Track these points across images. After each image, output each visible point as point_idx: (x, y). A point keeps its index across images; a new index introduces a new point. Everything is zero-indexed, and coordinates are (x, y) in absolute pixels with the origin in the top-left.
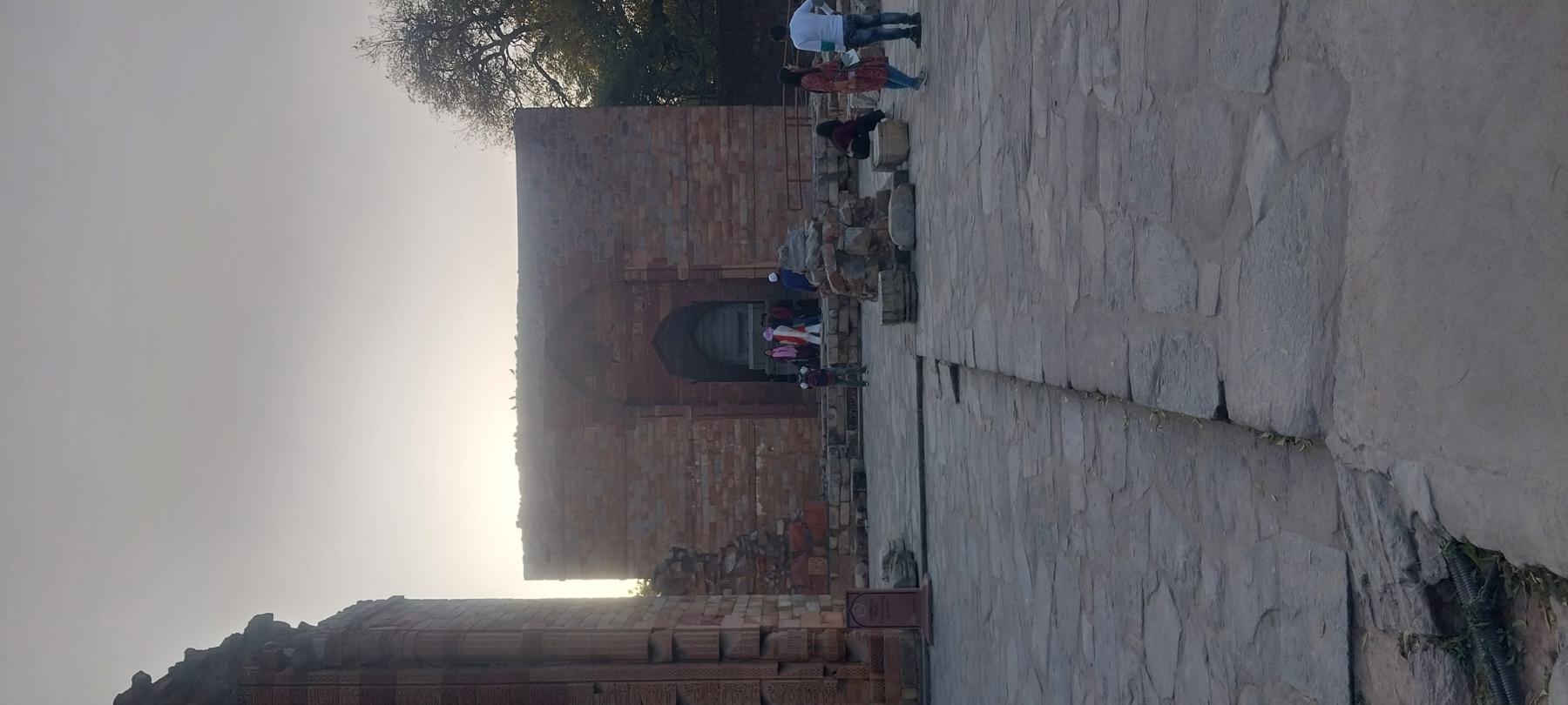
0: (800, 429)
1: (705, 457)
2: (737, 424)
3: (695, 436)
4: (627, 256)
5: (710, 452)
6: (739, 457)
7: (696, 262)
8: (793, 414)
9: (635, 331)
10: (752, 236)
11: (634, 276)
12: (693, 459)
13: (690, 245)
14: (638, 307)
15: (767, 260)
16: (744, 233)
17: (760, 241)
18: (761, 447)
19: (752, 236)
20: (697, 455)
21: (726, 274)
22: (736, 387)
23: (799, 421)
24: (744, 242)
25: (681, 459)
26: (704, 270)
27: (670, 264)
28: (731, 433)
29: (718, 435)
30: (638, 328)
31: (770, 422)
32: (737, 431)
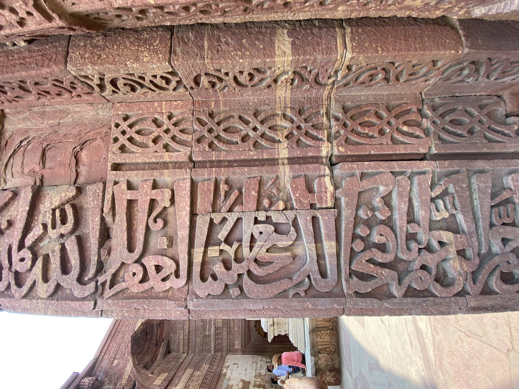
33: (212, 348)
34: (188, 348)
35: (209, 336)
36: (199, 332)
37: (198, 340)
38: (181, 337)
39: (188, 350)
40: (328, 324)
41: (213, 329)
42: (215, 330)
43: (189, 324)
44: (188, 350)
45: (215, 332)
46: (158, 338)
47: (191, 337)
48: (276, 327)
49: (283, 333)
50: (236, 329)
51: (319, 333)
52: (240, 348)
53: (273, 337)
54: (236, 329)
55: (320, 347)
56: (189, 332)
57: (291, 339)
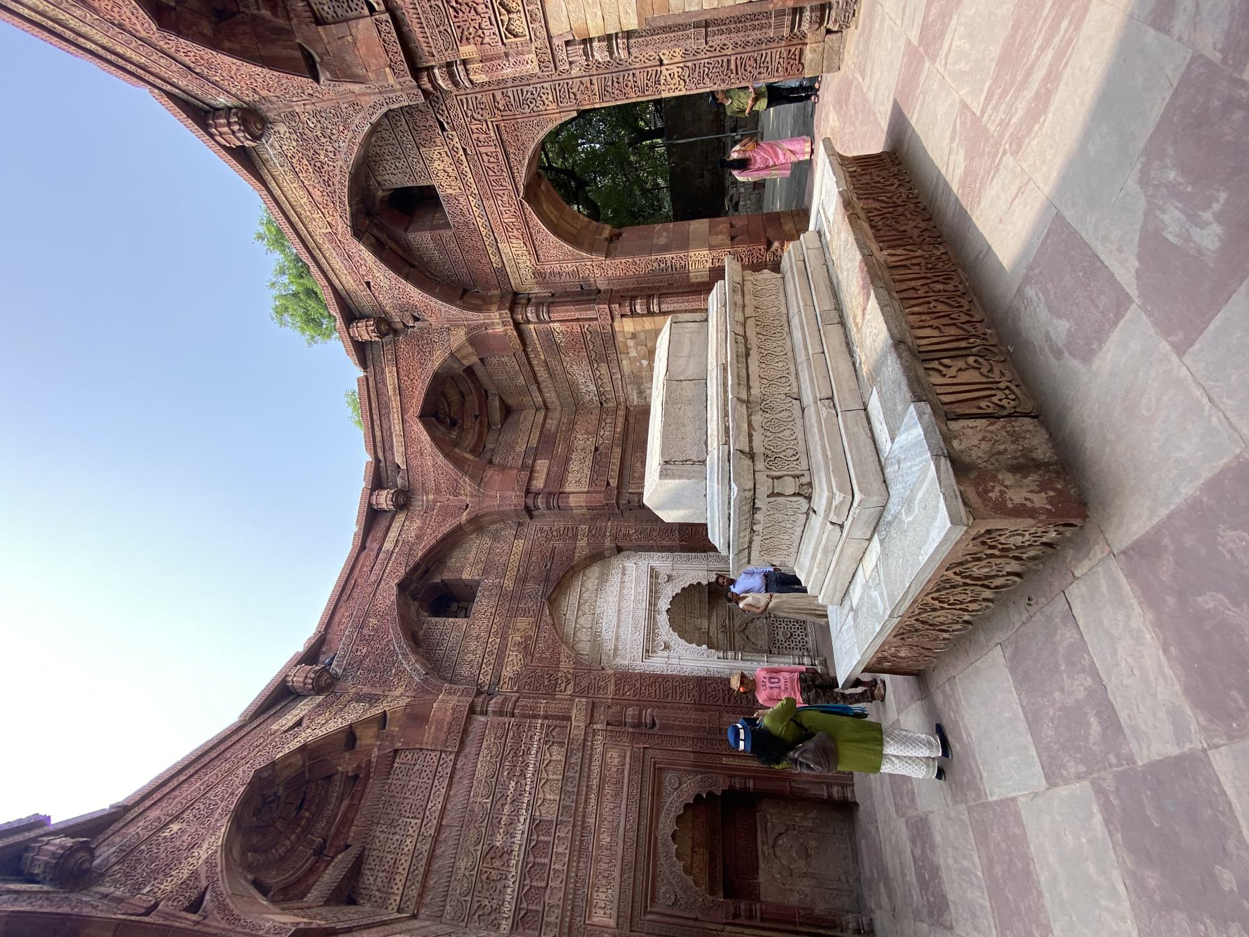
33: (508, 909)
34: (421, 895)
35: (507, 853)
36: (473, 835)
37: (462, 865)
38: (409, 844)
39: (419, 904)
41: (522, 827)
42: (530, 832)
43: (447, 798)
44: (419, 904)
45: (529, 840)
46: (333, 830)
47: (438, 852)
50: (606, 839)
52: (612, 923)
54: (606, 839)
56: (440, 827)
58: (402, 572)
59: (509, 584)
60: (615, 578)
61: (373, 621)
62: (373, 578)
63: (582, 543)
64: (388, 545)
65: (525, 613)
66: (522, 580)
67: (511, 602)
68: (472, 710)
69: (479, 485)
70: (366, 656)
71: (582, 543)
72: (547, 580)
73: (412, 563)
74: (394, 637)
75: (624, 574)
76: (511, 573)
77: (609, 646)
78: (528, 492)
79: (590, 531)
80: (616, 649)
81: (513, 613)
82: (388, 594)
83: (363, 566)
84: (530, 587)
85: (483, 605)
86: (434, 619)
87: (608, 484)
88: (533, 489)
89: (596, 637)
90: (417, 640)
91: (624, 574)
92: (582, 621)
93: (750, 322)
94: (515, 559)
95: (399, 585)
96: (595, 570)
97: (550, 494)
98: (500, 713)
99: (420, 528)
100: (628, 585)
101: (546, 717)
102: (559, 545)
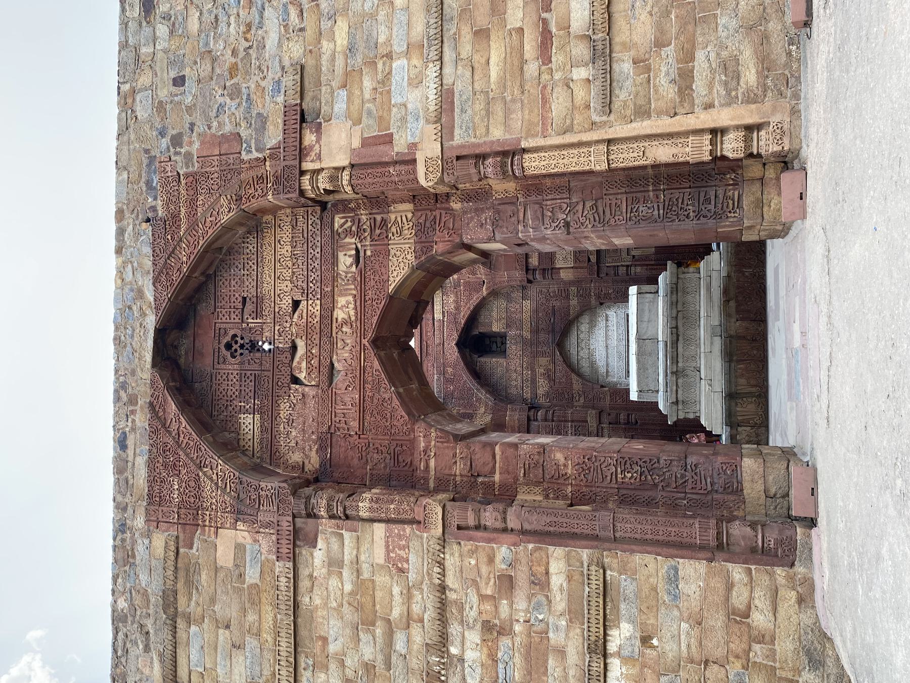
0: (739, 598)
1: (474, 637)
2: (558, 562)
3: (450, 581)
4: (309, 138)
5: (487, 627)
6: (561, 653)
7: (460, 138)
8: (718, 549)
9: (339, 314)
10: (602, 53)
11: (323, 184)
12: (444, 640)
13: (446, 98)
14: (345, 260)
15: (642, 112)
16: (581, 50)
17: (624, 66)
18: (621, 636)
19: (602, 53)
20: (454, 629)
21: (534, 164)
22: (562, 451)
23: (737, 572)
24: (580, 73)
25: (418, 636)
26: (481, 157)
27: (400, 145)
28: (541, 583)
29: (507, 583)
30: (345, 307)
31: (651, 567)
32: (557, 580)
40: (753, 390)
48: (680, 407)
49: (691, 416)
51: (740, 401)
53: (675, 419)
55: (739, 418)
57: (703, 422)
58: (455, 336)
59: (527, 334)
60: (602, 323)
61: (450, 370)
62: (437, 341)
63: (574, 302)
64: (438, 316)
65: (543, 354)
66: (536, 331)
67: (532, 347)
68: (529, 419)
69: (490, 268)
70: (454, 391)
71: (574, 302)
72: (553, 331)
73: (460, 329)
74: (466, 377)
75: (607, 320)
76: (527, 326)
77: (603, 370)
78: (527, 270)
79: (578, 292)
80: (607, 372)
81: (535, 355)
82: (452, 353)
83: (427, 332)
84: (543, 336)
85: (513, 348)
86: (483, 359)
87: (589, 260)
88: (531, 267)
89: (593, 364)
90: (477, 374)
91: (607, 320)
92: (581, 354)
93: (680, 315)
94: (526, 316)
95: (456, 344)
96: (585, 319)
97: (544, 270)
98: (546, 420)
99: (456, 302)
100: (611, 328)
101: (572, 421)
102: (557, 304)
